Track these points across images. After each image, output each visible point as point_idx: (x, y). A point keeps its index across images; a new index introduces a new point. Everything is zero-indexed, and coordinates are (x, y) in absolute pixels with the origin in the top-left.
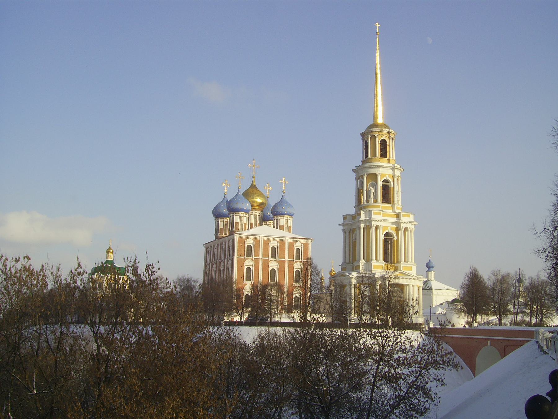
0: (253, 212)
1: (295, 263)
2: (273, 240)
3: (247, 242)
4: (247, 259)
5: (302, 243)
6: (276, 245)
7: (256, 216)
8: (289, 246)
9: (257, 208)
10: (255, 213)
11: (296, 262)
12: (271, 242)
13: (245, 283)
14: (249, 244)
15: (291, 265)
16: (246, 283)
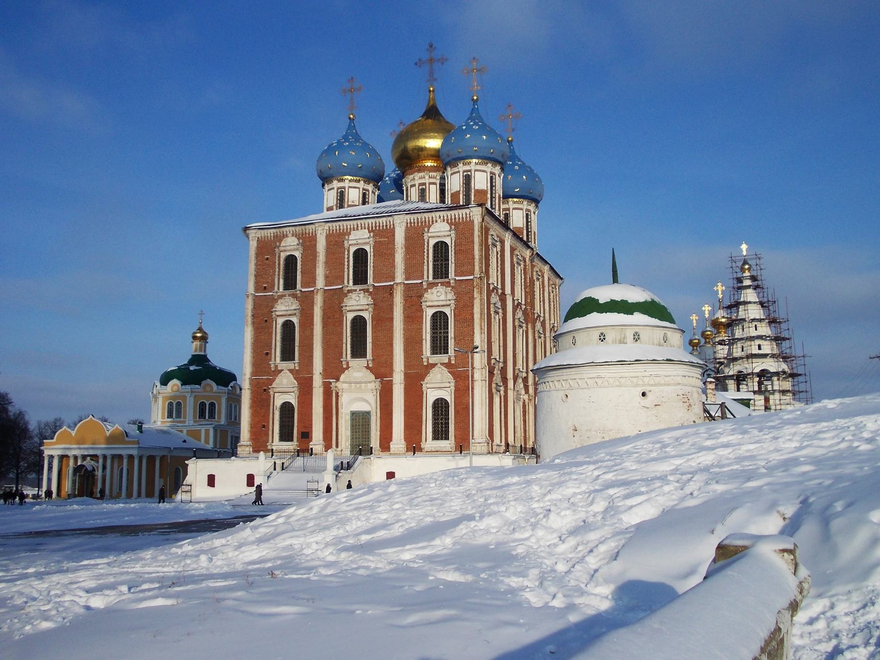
0: (414, 179)
1: (426, 290)
2: (358, 229)
3: (282, 249)
4: (281, 297)
5: (451, 224)
6: (365, 243)
7: (424, 187)
8: (407, 238)
9: (429, 164)
10: (421, 178)
11: (431, 285)
12: (352, 237)
13: (276, 367)
14: (288, 253)
15: (415, 299)
16: (280, 368)
